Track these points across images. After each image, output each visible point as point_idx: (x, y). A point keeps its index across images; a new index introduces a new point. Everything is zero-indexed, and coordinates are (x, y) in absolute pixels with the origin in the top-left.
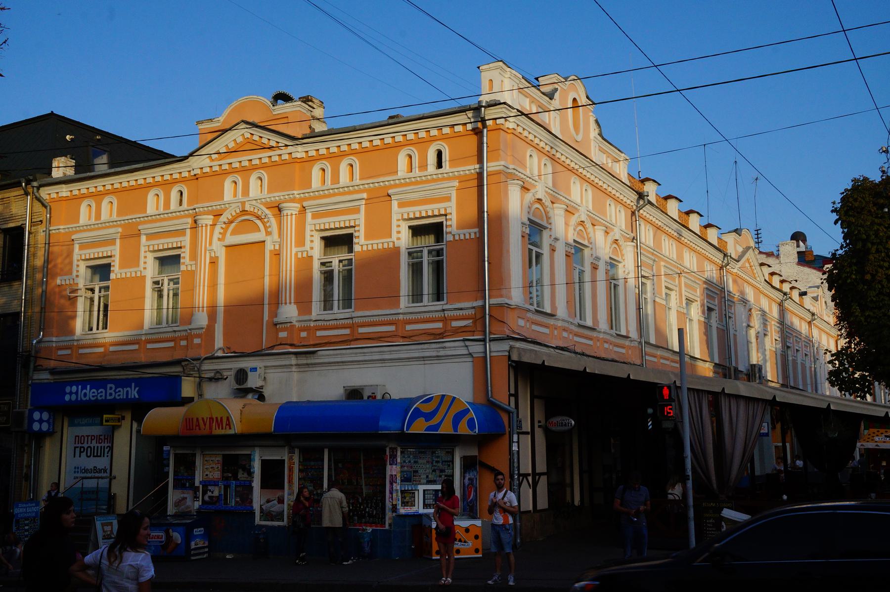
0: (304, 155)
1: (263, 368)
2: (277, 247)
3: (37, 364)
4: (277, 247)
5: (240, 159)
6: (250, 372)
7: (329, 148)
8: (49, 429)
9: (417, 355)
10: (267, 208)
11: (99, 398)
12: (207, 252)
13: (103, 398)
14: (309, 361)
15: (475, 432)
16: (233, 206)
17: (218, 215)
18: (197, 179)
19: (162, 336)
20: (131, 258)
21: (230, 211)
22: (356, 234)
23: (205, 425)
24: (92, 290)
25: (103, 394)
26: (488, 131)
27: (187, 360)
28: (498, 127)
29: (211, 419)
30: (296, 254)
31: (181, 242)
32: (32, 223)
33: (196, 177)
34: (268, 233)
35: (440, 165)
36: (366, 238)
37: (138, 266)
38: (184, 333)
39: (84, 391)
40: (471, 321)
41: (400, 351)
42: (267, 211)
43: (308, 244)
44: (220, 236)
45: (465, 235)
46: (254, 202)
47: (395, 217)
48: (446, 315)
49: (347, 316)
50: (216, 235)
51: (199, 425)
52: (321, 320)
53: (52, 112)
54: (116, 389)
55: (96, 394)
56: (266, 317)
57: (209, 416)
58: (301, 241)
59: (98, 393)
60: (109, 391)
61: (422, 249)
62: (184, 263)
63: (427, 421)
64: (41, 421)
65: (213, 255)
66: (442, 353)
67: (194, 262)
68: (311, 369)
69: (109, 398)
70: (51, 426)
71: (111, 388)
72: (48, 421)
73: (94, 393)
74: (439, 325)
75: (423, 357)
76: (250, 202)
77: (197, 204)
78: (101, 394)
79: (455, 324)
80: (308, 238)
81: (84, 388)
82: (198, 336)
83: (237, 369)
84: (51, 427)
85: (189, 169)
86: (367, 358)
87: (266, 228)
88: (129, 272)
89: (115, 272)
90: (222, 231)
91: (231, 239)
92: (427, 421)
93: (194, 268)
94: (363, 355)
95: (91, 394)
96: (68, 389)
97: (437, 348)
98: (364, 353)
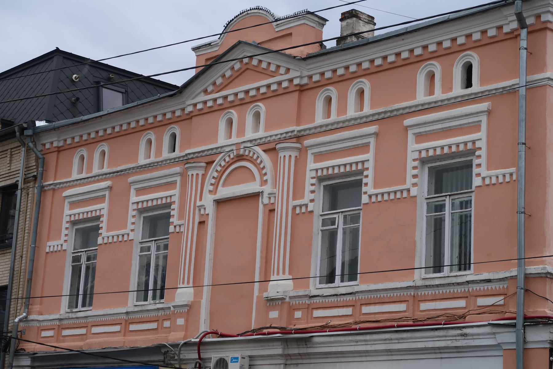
0: (305, 81)
1: (247, 359)
3: (19, 348)
4: (272, 201)
6: (231, 362)
9: (430, 345)
10: (264, 151)
14: (303, 351)
17: (209, 163)
18: (191, 118)
19: (145, 315)
22: (365, 181)
26: (529, 33)
27: (165, 346)
28: (543, 26)
31: (171, 196)
32: (26, 181)
33: (190, 117)
35: (468, 83)
36: (376, 185)
37: (126, 227)
40: (502, 297)
41: (411, 338)
42: (264, 156)
43: (308, 196)
44: (211, 188)
45: (497, 177)
46: (249, 145)
47: (411, 156)
49: (349, 290)
50: (208, 187)
52: (318, 296)
58: (298, 192)
61: (444, 198)
62: (173, 222)
65: (202, 212)
66: (462, 343)
68: (304, 361)
74: (462, 303)
75: (439, 348)
77: (189, 148)
79: (481, 301)
80: (308, 188)
82: (180, 315)
83: (219, 358)
85: (182, 106)
86: (369, 348)
89: (103, 235)
90: (213, 181)
91: (224, 192)
94: (364, 343)
97: (456, 336)
98: (365, 341)
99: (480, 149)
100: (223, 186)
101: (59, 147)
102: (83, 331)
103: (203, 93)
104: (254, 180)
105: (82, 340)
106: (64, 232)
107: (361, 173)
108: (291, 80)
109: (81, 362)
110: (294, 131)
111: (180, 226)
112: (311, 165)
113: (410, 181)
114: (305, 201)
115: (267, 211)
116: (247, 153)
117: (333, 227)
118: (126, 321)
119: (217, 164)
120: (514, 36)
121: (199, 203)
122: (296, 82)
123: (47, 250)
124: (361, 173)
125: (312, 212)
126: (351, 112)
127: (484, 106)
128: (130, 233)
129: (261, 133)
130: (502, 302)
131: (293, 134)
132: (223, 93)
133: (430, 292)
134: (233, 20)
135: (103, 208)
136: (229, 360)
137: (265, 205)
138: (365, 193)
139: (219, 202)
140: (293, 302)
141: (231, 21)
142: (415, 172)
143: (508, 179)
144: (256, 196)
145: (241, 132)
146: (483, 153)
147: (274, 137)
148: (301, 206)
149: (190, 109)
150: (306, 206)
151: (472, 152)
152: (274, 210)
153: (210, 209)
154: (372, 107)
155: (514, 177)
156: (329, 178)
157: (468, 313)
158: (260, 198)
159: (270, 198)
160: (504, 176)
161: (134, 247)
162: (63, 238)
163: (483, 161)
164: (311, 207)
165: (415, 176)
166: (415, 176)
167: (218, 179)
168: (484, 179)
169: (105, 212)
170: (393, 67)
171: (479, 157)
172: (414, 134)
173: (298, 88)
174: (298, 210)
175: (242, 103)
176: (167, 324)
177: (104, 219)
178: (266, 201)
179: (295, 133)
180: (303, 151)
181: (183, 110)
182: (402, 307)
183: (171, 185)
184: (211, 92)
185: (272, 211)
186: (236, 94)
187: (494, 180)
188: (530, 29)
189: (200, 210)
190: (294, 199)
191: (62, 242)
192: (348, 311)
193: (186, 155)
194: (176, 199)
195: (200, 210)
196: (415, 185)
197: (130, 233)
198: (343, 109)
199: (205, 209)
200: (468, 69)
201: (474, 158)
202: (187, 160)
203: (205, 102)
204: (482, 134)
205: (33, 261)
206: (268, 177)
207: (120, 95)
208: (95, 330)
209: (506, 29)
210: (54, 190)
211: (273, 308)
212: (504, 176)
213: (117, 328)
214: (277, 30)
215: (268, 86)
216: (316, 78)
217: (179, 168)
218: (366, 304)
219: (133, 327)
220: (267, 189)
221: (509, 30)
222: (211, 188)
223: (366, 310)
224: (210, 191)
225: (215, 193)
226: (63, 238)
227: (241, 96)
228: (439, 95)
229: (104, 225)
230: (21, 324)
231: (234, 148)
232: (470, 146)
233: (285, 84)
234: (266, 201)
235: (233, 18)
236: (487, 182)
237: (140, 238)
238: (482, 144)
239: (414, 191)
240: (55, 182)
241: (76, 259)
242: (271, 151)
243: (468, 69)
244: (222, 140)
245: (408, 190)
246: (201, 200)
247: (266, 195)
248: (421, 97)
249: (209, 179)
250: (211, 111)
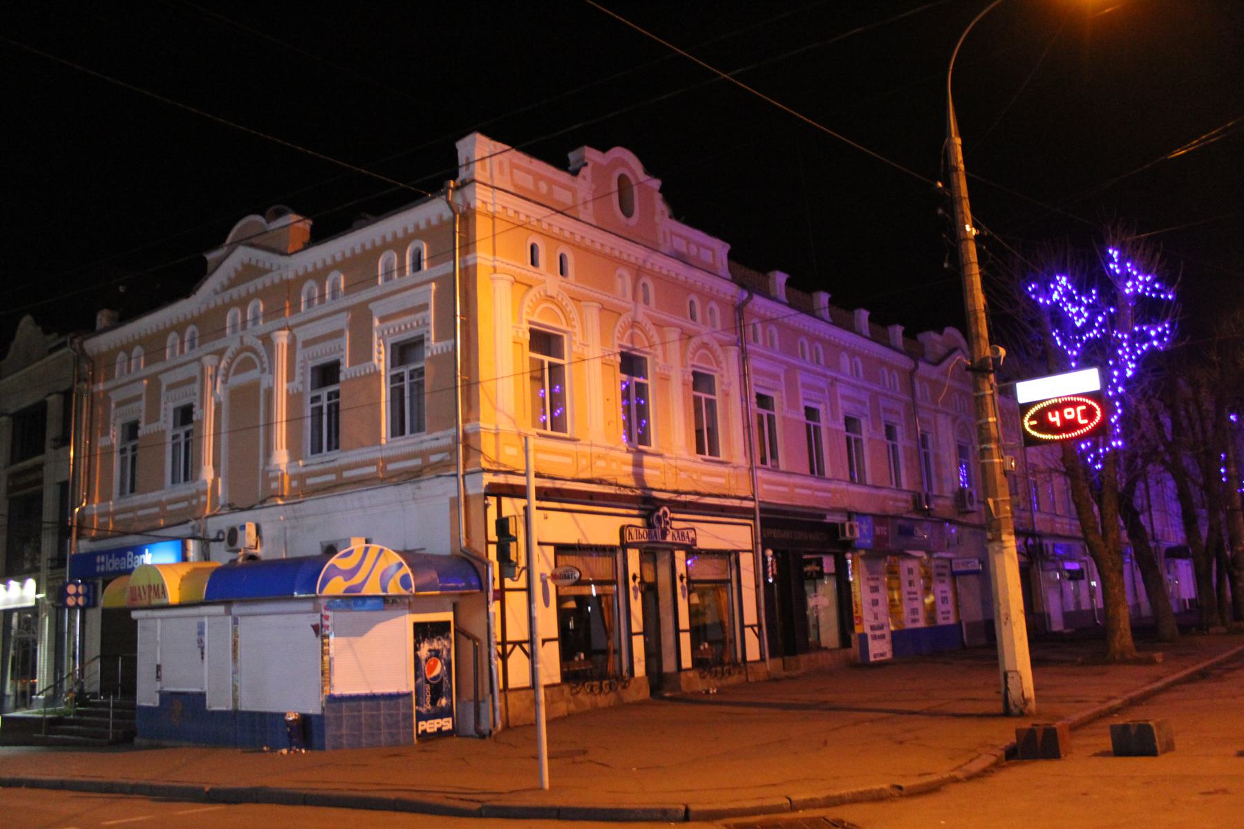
15: (411, 592)
23: (145, 593)
29: (150, 586)
39: (111, 561)
51: (140, 595)
56: (261, 467)
57: (148, 584)
63: (346, 580)
64: (77, 595)
71: (130, 556)
79: (434, 458)
81: (110, 557)
84: (91, 601)
88: (154, 427)
92: (346, 580)
96: (98, 560)
104: (255, 367)
130: (449, 458)
136: (238, 529)
157: (425, 467)
176: (194, 502)
208: (140, 513)
241: (123, 451)
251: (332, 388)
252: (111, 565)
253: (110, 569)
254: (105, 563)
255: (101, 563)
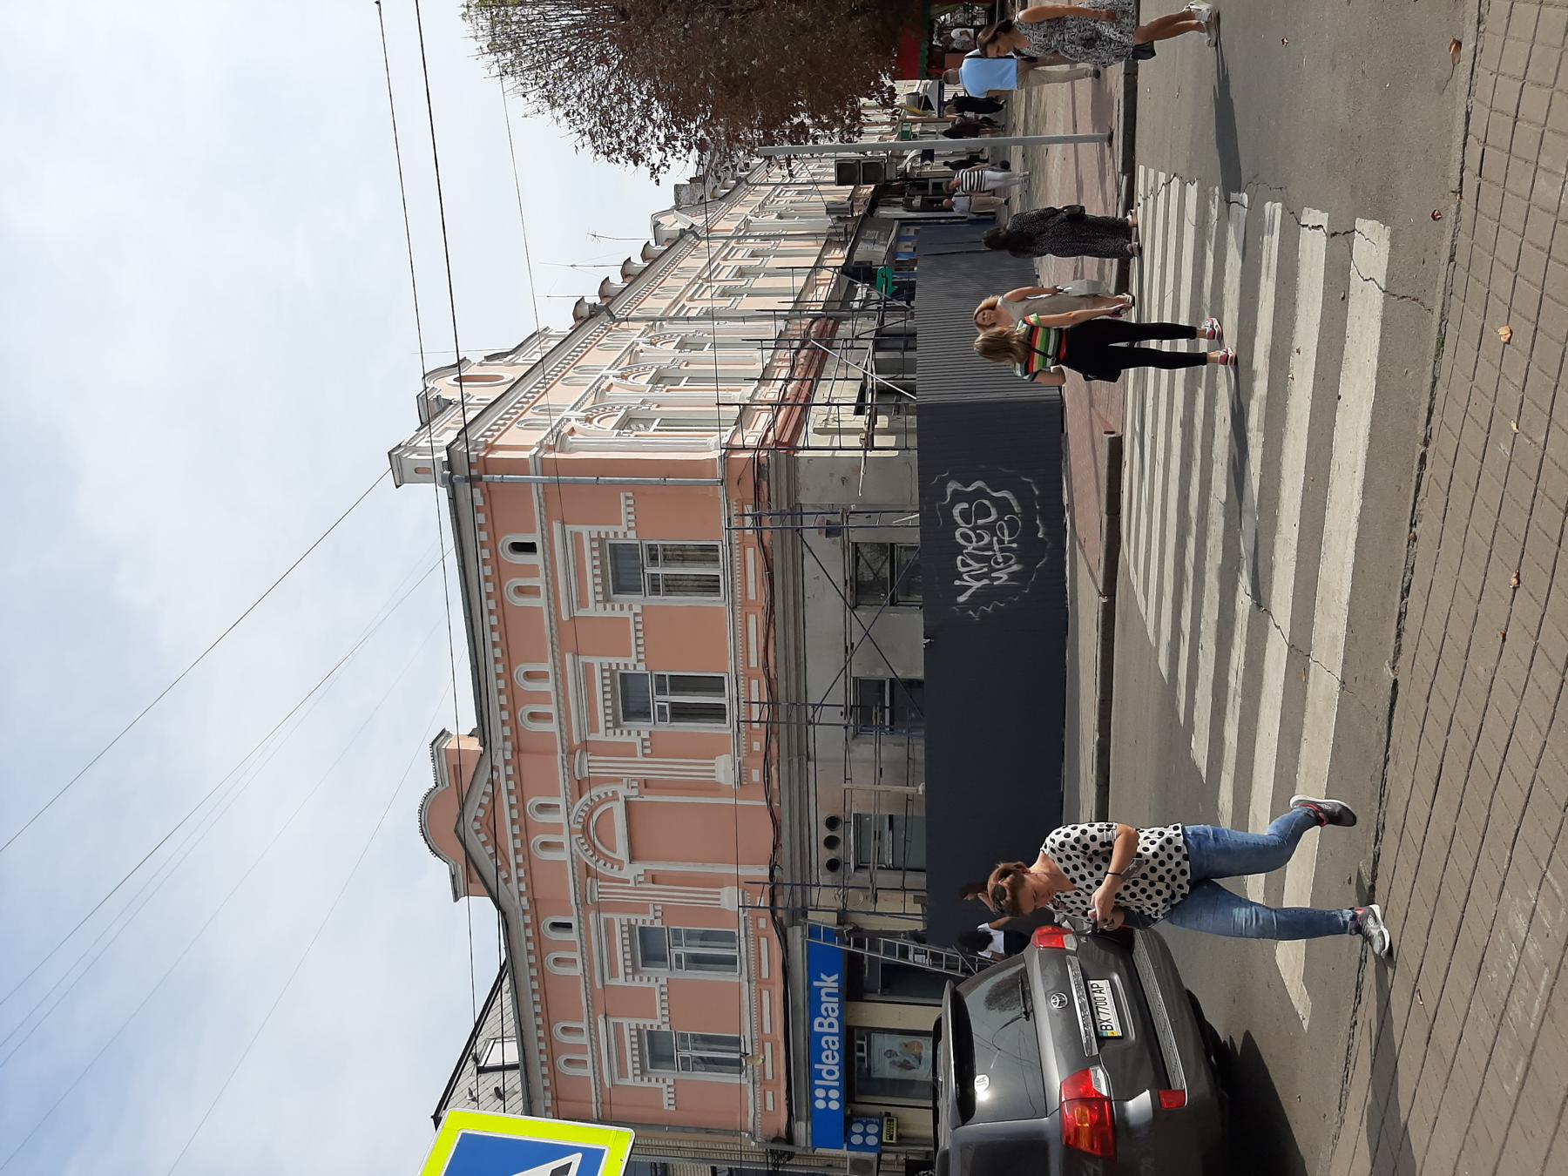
0: (508, 745)
2: (635, 784)
4: (635, 784)
5: (510, 837)
7: (501, 705)
8: (876, 1124)
10: (580, 797)
11: (837, 1046)
12: (638, 886)
13: (836, 1039)
16: (575, 846)
18: (534, 899)
20: (640, 1001)
21: (582, 852)
24: (685, 1060)
25: (830, 1039)
30: (645, 755)
31: (622, 926)
33: (533, 901)
34: (615, 797)
35: (530, 548)
38: (749, 922)
42: (586, 797)
43: (634, 739)
45: (629, 513)
46: (572, 817)
47: (600, 613)
48: (737, 542)
50: (615, 873)
53: (432, 1117)
54: (822, 1016)
55: (830, 1052)
58: (628, 750)
59: (829, 1049)
60: (826, 1029)
61: (646, 577)
62: (651, 921)
64: (865, 1134)
67: (651, 907)
69: (836, 1030)
70: (872, 1119)
72: (865, 1125)
73: (827, 1057)
76: (571, 822)
78: (830, 1043)
80: (625, 739)
84: (875, 1121)
85: (521, 912)
87: (608, 800)
89: (660, 1024)
91: (622, 852)
93: (659, 908)
95: (830, 1061)
99: (599, 533)
100: (615, 852)
101: (553, 1099)
102: (768, 1046)
103: (508, 885)
105: (778, 1049)
106: (653, 1084)
107: (613, 673)
108: (507, 763)
109: (803, 1046)
110: (562, 757)
111: (656, 911)
112: (600, 736)
113: (627, 614)
114: (638, 741)
115: (646, 790)
116: (581, 820)
117: (667, 708)
118: (758, 983)
119: (590, 861)
120: (488, 494)
121: (632, 884)
122: (508, 756)
123: (673, 1108)
124: (613, 673)
125: (650, 733)
126: (548, 686)
127: (556, 527)
128: (660, 982)
129: (561, 802)
131: (565, 758)
132: (511, 852)
133: (738, 588)
134: (429, 845)
135: (629, 1024)
137: (640, 795)
138: (635, 668)
139: (633, 858)
140: (743, 752)
141: (430, 848)
142: (617, 607)
143: (631, 502)
144: (627, 803)
145: (556, 829)
146: (603, 529)
147: (567, 784)
148: (644, 747)
149: (524, 900)
150: (644, 740)
151: (601, 541)
152: (645, 780)
153: (639, 868)
154: (545, 661)
155: (630, 494)
156: (615, 714)
158: (632, 799)
159: (632, 787)
160: (629, 506)
161: (680, 977)
162: (660, 1085)
163: (611, 529)
164: (645, 735)
165: (622, 608)
166: (622, 608)
167: (608, 859)
168: (629, 529)
169: (633, 1022)
170: (505, 636)
171: (607, 533)
172: (578, 609)
173: (515, 754)
174: (648, 751)
175: (525, 828)
177: (641, 1022)
178: (635, 792)
179: (564, 755)
180: (585, 746)
181: (524, 912)
182: (752, 619)
183: (609, 923)
184: (510, 875)
185: (646, 783)
186: (515, 836)
187: (632, 517)
188: (483, 472)
189: (640, 882)
190: (636, 756)
191: (664, 1086)
192: (754, 683)
193: (577, 904)
194: (624, 917)
195: (640, 882)
196: (630, 608)
197: (660, 982)
198: (543, 697)
199: (638, 875)
200: (519, 548)
201: (608, 542)
202: (583, 903)
203: (519, 880)
204: (584, 530)
205: (684, 1129)
206: (609, 789)
207: (496, 1044)
208: (767, 1030)
209: (479, 502)
210: (603, 1103)
211: (749, 774)
212: (629, 506)
213: (765, 994)
214: (448, 784)
215: (510, 792)
216: (507, 731)
217: (590, 915)
218: (748, 663)
219: (765, 975)
220: (622, 790)
221: (482, 499)
222: (616, 867)
223: (753, 664)
224: (619, 870)
225: (623, 862)
226: (660, 1085)
227: (517, 831)
228: (539, 582)
229: (648, 1022)
230: (759, 1139)
231: (574, 837)
232: (595, 545)
233: (510, 770)
234: (635, 792)
235: (426, 845)
236: (632, 525)
237: (666, 970)
238: (594, 530)
239: (637, 609)
240: (594, 1100)
242: (581, 786)
243: (519, 548)
244: (563, 856)
245: (636, 615)
246: (628, 882)
247: (629, 793)
248: (540, 602)
249: (606, 870)
250: (529, 872)
251: (652, 687)
252: (831, 1073)
253: (837, 1075)
254: (827, 1089)
255: (827, 1099)
